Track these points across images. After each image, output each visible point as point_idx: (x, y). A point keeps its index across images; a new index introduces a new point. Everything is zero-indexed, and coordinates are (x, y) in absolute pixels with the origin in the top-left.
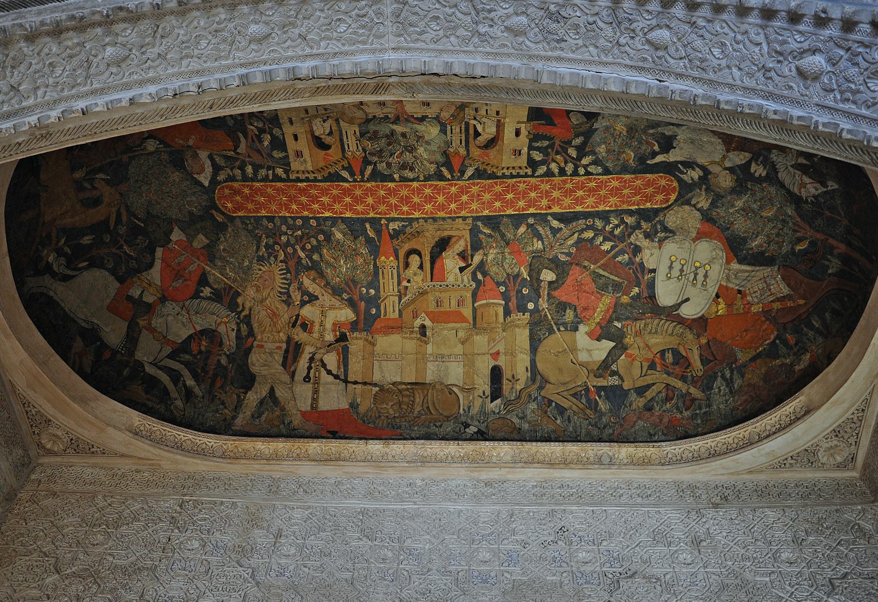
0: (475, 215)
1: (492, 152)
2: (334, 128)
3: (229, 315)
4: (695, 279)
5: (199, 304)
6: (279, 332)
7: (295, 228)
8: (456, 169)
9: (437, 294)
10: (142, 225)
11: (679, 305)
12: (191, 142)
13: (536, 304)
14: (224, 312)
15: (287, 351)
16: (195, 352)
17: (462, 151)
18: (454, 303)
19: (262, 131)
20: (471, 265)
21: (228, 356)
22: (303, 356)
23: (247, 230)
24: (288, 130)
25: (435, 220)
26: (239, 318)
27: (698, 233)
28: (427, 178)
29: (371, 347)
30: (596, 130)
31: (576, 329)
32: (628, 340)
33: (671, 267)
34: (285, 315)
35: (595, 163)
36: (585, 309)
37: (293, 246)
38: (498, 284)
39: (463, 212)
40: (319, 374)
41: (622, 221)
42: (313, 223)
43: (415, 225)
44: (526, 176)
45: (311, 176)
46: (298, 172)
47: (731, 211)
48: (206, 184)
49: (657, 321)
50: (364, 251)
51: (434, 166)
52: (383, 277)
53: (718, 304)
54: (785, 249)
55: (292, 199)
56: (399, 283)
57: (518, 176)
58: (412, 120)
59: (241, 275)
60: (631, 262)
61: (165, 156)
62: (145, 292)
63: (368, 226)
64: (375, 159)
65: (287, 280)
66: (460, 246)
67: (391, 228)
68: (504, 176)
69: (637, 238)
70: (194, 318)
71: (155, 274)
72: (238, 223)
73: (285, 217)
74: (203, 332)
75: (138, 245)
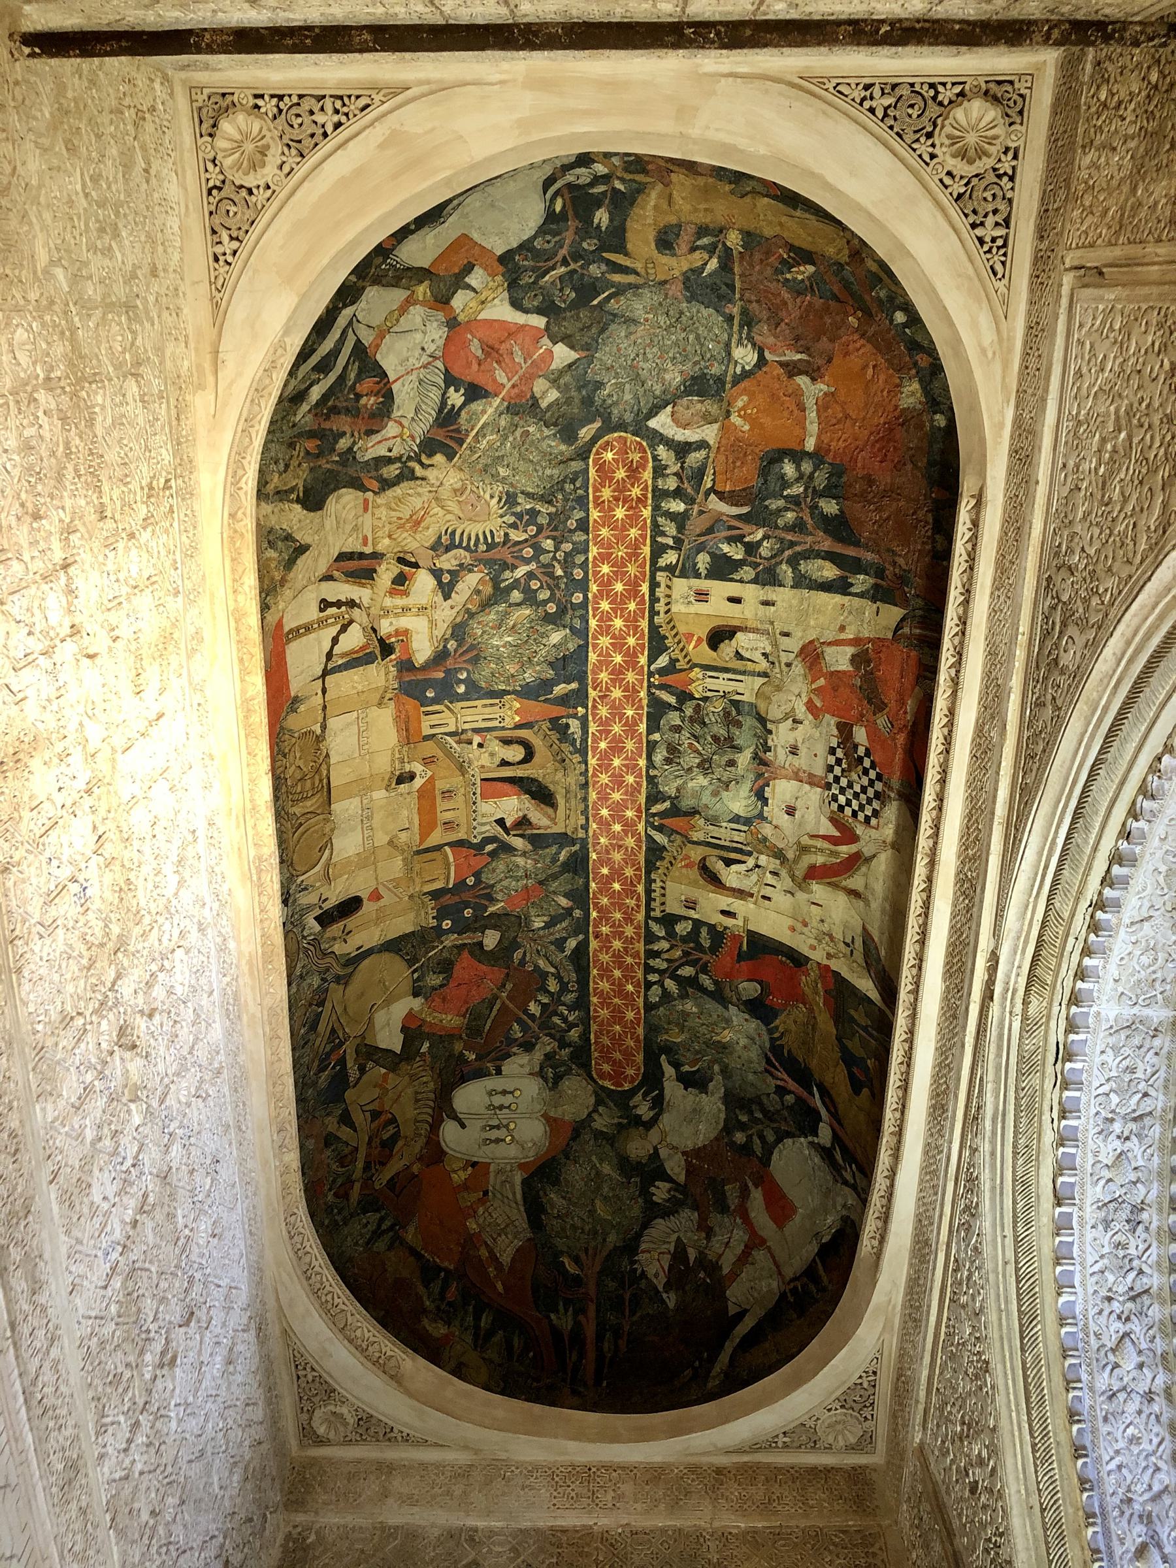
0: (590, 840)
1: (694, 873)
2: (750, 666)
3: (413, 439)
4: (492, 1127)
5: (434, 384)
6: (390, 536)
7: (567, 563)
8: (666, 822)
9: (462, 790)
10: (595, 302)
11: (455, 1117)
12: (735, 419)
13: (450, 931)
14: (420, 429)
15: (362, 556)
16: (358, 388)
17: (696, 836)
18: (448, 816)
19: (752, 549)
20: (508, 833)
21: (350, 449)
22: (356, 588)
23: (564, 481)
24: (751, 593)
25: (585, 786)
26: (409, 458)
27: (555, 1120)
28: (651, 780)
29: (376, 701)
30: (727, 1008)
31: (416, 994)
32: (404, 1067)
33: (504, 1092)
34: (416, 543)
35: (666, 995)
36: (444, 1000)
37: (535, 557)
38: (477, 875)
39: (595, 826)
40: (332, 624)
41: (571, 1026)
42: (578, 598)
43: (577, 758)
44: (649, 909)
45: (660, 607)
46: (669, 587)
47: (594, 1158)
48: (653, 423)
49: (432, 1096)
50: (529, 676)
51: (673, 793)
52: (485, 706)
53: (464, 1169)
54: (560, 1243)
55: (619, 568)
56: (476, 731)
57: (649, 900)
58: (761, 782)
59: (481, 461)
60: (511, 1042)
61: (716, 369)
62: (472, 294)
63: (574, 686)
64: (689, 712)
65: (476, 545)
66: (539, 818)
67: (570, 721)
68: (649, 882)
69: (546, 1045)
70: (414, 377)
71: (501, 311)
72: (576, 466)
73: (586, 551)
74: (389, 396)
75: (561, 290)
